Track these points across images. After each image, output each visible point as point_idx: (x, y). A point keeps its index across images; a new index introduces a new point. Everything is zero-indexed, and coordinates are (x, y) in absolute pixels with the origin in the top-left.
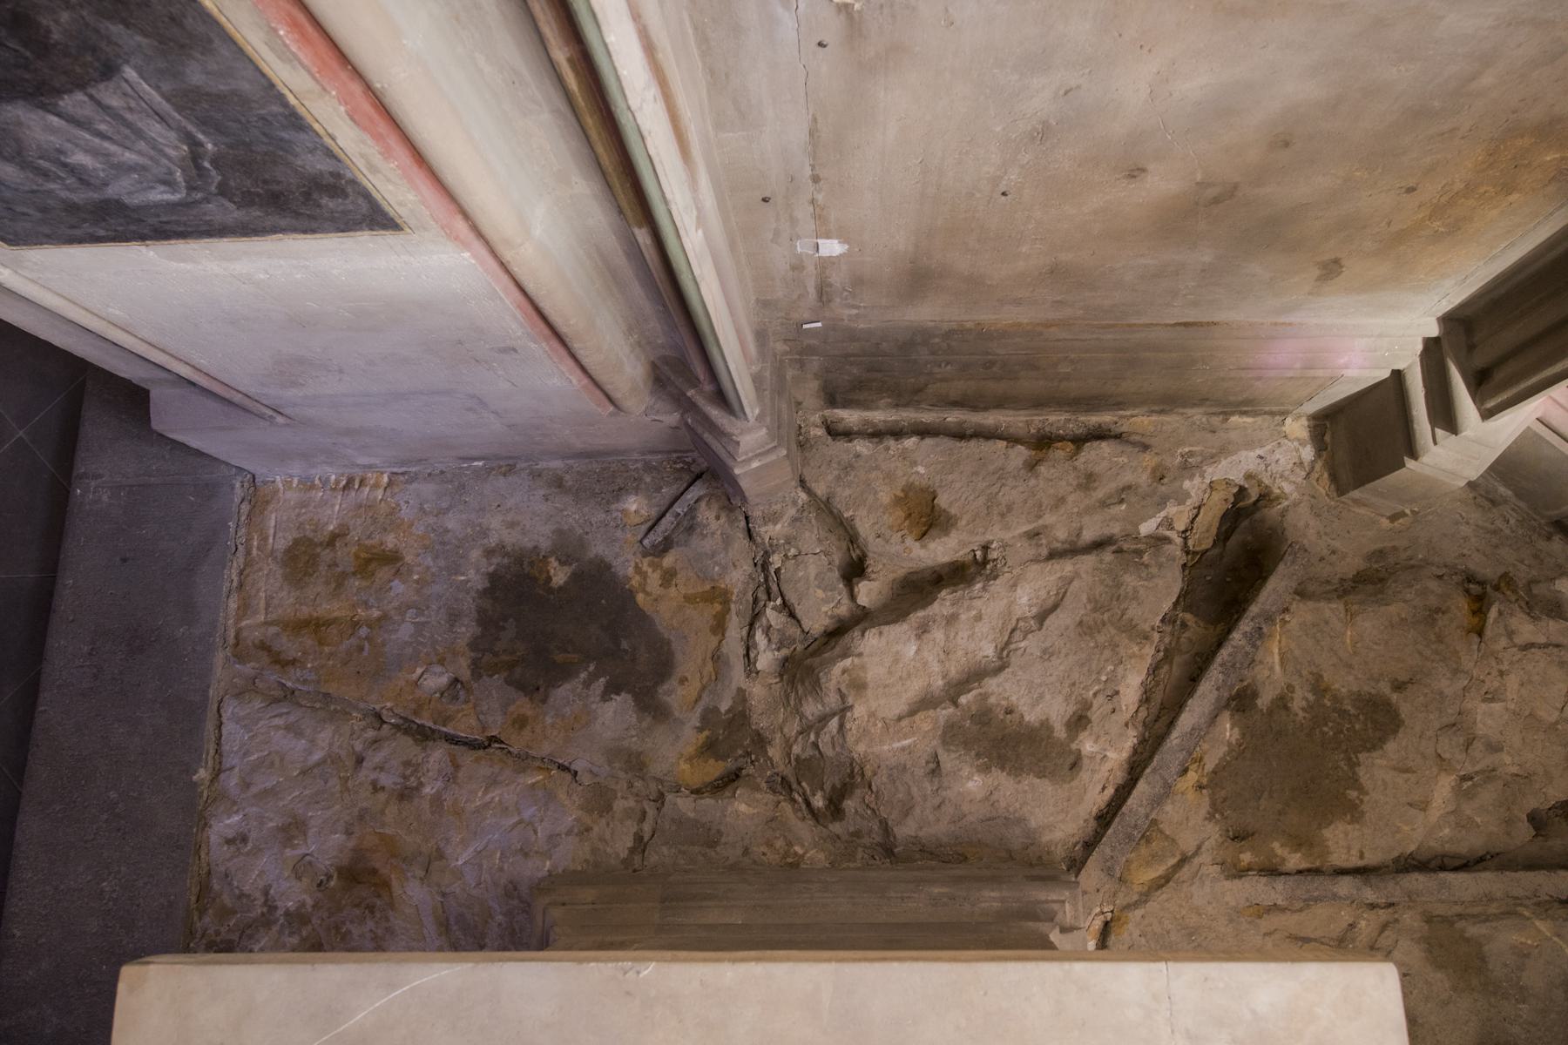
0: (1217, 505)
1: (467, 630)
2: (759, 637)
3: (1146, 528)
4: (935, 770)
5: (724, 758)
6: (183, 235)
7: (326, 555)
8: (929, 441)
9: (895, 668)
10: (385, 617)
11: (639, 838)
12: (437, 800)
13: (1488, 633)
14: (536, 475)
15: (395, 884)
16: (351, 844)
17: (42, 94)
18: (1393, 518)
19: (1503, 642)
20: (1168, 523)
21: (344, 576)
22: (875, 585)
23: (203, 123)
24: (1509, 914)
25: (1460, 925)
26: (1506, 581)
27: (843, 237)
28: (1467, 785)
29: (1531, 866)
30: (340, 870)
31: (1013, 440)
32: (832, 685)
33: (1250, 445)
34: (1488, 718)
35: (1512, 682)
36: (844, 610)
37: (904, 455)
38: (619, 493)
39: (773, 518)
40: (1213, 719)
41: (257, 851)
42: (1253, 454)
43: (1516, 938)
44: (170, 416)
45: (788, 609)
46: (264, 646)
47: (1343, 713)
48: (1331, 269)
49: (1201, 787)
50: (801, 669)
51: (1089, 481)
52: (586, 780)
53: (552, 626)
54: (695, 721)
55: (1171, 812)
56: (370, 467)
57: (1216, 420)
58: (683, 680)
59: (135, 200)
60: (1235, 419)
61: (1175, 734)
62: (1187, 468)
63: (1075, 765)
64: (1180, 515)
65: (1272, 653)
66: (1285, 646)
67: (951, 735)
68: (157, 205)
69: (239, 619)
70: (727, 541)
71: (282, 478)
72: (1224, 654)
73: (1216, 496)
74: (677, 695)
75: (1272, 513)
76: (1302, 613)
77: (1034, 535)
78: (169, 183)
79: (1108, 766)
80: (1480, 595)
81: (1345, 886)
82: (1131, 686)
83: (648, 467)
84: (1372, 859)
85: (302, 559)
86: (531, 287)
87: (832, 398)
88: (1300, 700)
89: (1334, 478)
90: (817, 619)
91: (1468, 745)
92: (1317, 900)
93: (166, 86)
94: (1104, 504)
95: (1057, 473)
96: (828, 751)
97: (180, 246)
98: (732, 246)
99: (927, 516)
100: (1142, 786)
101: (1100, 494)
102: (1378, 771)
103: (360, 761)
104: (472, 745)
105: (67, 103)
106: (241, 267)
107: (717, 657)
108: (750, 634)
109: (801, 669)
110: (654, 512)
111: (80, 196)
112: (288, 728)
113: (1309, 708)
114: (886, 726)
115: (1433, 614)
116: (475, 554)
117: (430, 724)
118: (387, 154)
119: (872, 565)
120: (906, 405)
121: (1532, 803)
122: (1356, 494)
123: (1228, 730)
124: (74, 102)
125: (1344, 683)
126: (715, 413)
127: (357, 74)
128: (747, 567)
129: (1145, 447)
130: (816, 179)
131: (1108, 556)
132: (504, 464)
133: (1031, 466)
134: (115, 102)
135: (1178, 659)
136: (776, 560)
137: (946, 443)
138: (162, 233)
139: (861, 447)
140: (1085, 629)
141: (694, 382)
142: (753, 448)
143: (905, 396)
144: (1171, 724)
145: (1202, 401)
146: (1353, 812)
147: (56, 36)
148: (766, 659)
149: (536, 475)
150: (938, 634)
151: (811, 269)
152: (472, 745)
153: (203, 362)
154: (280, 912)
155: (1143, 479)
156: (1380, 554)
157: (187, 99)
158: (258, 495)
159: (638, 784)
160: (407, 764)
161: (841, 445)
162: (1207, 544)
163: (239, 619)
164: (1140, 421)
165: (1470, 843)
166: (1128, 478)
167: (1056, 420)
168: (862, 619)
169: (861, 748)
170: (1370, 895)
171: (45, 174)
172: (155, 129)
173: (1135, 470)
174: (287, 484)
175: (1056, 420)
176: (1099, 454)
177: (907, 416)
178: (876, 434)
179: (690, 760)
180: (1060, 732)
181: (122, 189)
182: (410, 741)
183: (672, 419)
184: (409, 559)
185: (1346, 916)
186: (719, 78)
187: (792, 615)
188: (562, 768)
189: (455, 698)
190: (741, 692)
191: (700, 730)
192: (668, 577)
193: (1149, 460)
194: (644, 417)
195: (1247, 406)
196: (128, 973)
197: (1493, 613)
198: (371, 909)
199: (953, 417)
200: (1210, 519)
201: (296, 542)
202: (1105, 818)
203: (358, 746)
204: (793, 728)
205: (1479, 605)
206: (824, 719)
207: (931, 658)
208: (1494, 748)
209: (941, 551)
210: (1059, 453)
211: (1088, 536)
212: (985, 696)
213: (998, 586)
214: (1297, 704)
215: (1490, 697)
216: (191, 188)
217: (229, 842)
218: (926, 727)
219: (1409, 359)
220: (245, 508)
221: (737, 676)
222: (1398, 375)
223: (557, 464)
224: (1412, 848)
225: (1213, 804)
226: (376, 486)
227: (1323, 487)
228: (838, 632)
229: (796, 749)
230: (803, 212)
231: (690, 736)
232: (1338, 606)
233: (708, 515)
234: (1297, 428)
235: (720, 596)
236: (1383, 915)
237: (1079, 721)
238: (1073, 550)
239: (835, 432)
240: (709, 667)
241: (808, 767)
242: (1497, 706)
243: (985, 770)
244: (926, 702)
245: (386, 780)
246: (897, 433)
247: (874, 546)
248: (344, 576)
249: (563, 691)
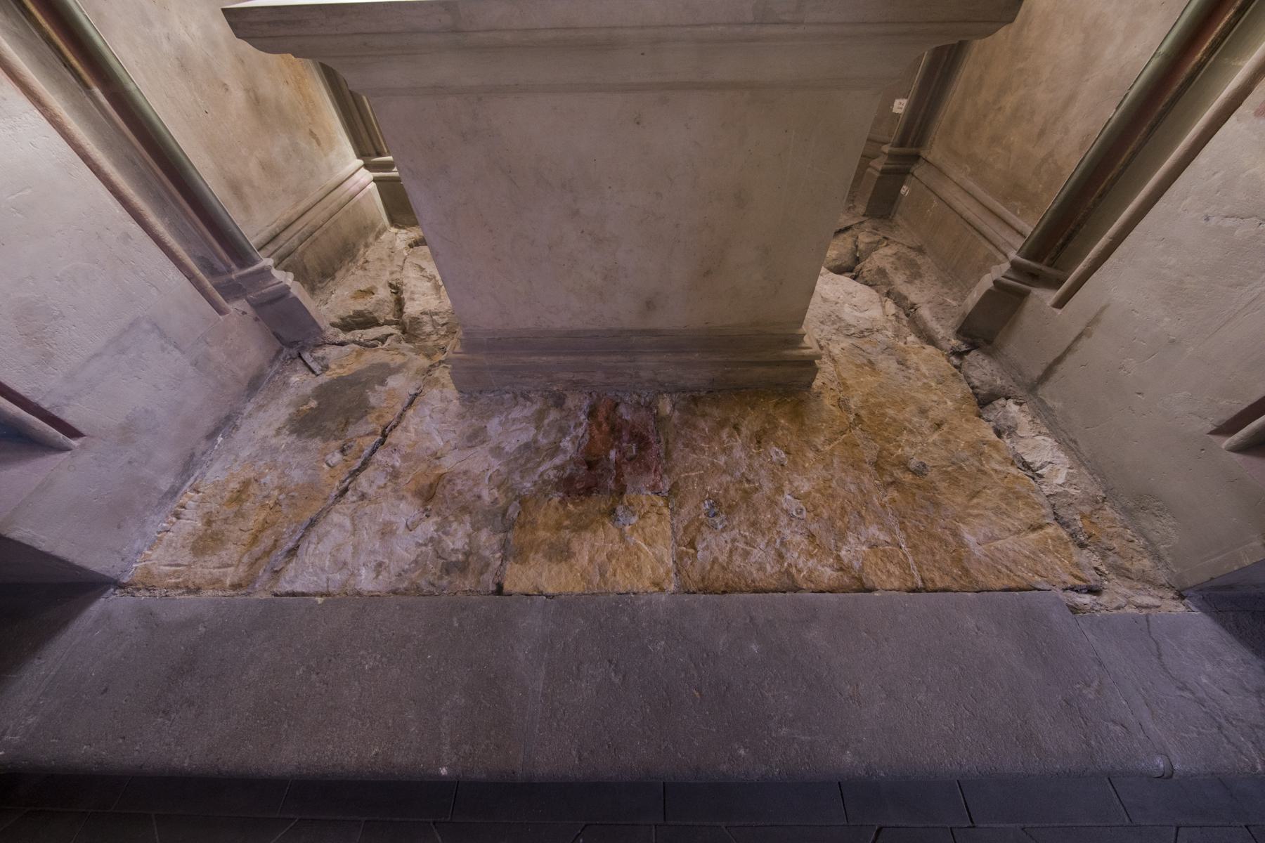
12: (405, 458)
15: (441, 472)
16: (410, 498)
30: (424, 505)
41: (391, 554)
154: (435, 535)
188: (411, 403)
198: (450, 481)
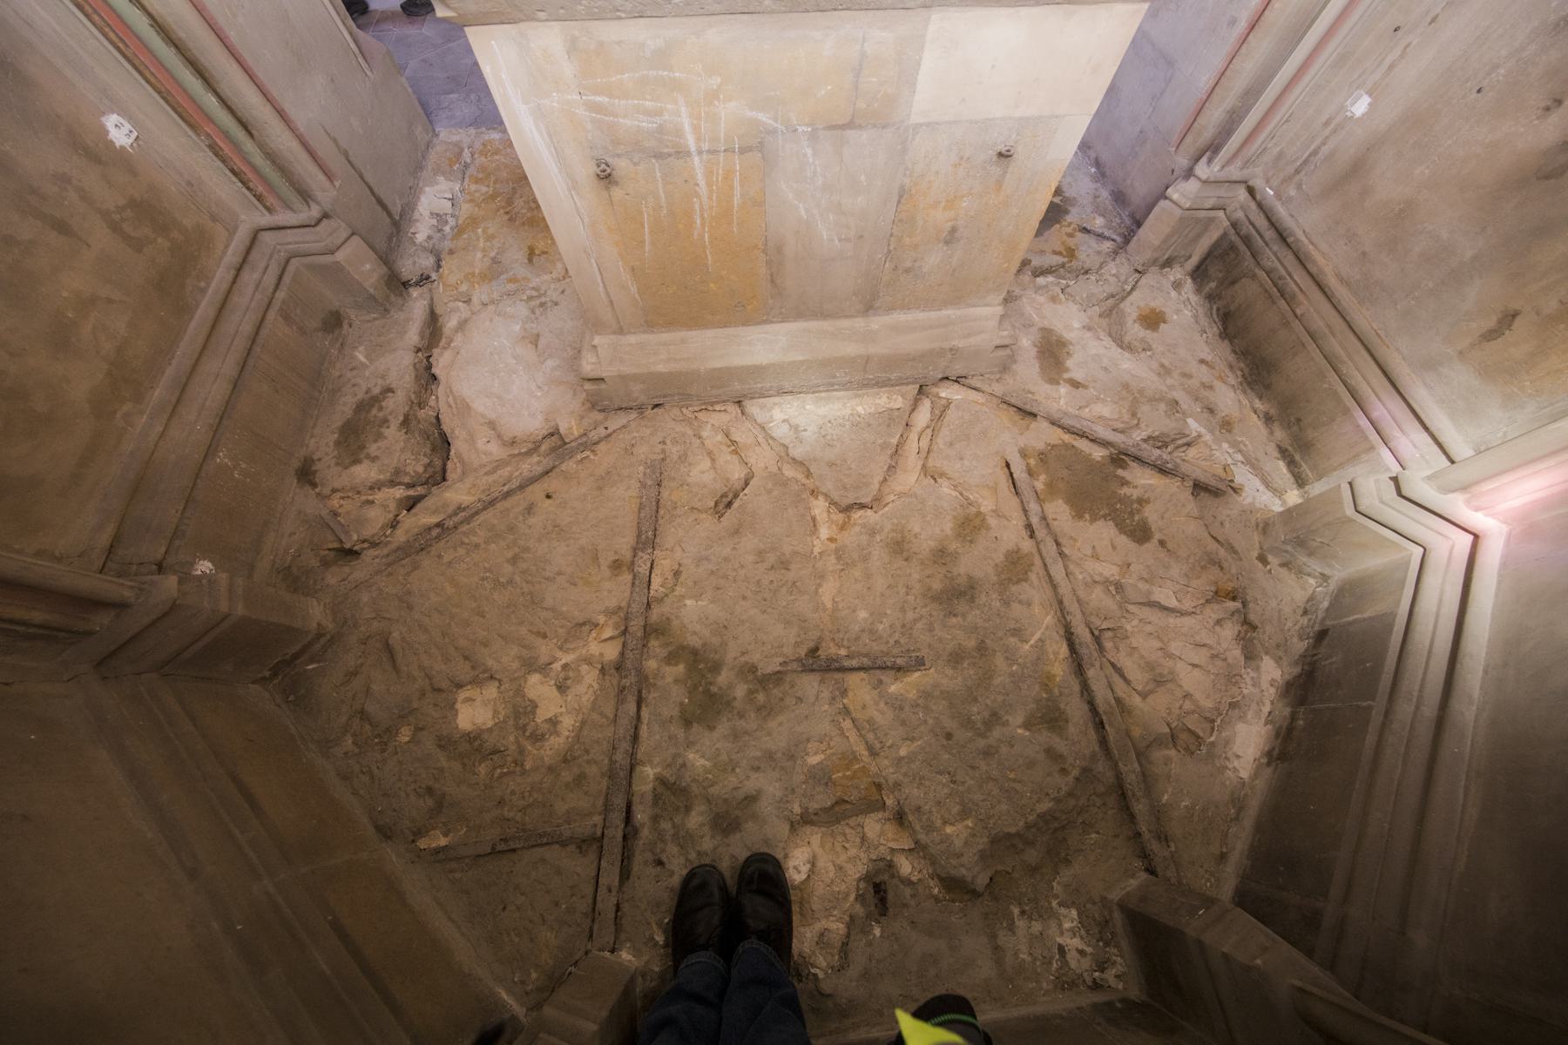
19: (1215, 616)
47: (1132, 514)
60: (1282, 464)
102: (1102, 533)
146: (1079, 515)
150: (1088, 334)
180: (1066, 376)
237: (1075, 384)
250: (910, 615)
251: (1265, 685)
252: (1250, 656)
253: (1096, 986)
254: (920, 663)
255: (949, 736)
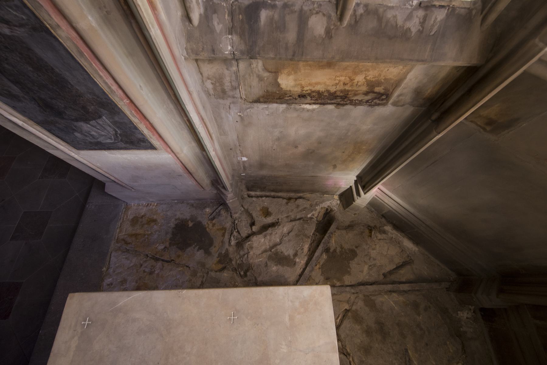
0: (323, 212)
1: (169, 236)
2: (232, 238)
3: (309, 216)
4: (266, 265)
5: (222, 264)
6: (113, 149)
7: (140, 220)
8: (268, 198)
9: (260, 244)
10: (152, 233)
11: (202, 282)
12: (158, 274)
13: (372, 237)
14: (188, 204)
17: (86, 121)
18: (355, 214)
20: (313, 215)
21: (144, 224)
22: (256, 227)
23: (118, 127)
24: (380, 294)
25: (370, 297)
26: (375, 227)
27: (246, 157)
28: (371, 267)
29: (383, 284)
31: (284, 198)
32: (246, 248)
33: (328, 200)
34: (373, 253)
35: (378, 247)
36: (250, 232)
37: (263, 201)
38: (205, 207)
39: (236, 213)
40: (321, 254)
42: (329, 202)
43: (381, 299)
44: (110, 189)
45: (238, 232)
46: (123, 240)
48: (335, 167)
49: (319, 268)
50: (240, 245)
51: (298, 206)
52: (192, 269)
53: (188, 235)
54: (217, 255)
55: (314, 273)
56: (153, 201)
57: (322, 195)
58: (215, 247)
59: (104, 142)
60: (325, 195)
61: (314, 257)
62: (317, 204)
63: (295, 264)
64: (316, 213)
65: (333, 241)
66: (335, 239)
67: (270, 258)
68: (108, 143)
69: (119, 234)
70: (226, 218)
71: (133, 204)
72: (323, 241)
73: (323, 210)
74: (213, 250)
75: (333, 213)
76: (338, 233)
77: (287, 217)
78: (111, 139)
79: (301, 264)
80: (371, 229)
81: (348, 289)
82: (306, 247)
83: (211, 202)
84: (353, 283)
85: (135, 221)
86: (183, 162)
87: (249, 189)
88: (338, 250)
89: (343, 207)
90: (244, 233)
91: (370, 259)
92: (343, 292)
93: (111, 120)
94: (301, 211)
95: (292, 205)
96: (245, 262)
97: (112, 151)
98: (225, 158)
99: (266, 213)
100: (308, 268)
101: (300, 209)
102: (353, 264)
103: (141, 265)
104: (167, 262)
105: (91, 122)
106: (125, 156)
107: (223, 242)
108: (230, 237)
109: (240, 245)
110: (212, 211)
111: (93, 141)
112: (126, 258)
113: (340, 252)
114: (257, 256)
115: (362, 233)
116: (173, 220)
117: (158, 257)
118: (154, 135)
119: (256, 223)
120: (263, 191)
121: (383, 271)
122: (347, 209)
123: (325, 256)
124: (93, 122)
125: (347, 246)
126: (223, 190)
127: (148, 120)
128: (230, 223)
129: (309, 200)
130: (240, 146)
131: (301, 221)
132: (181, 201)
133: (287, 203)
134: (101, 123)
135: (315, 242)
136: (236, 222)
137: (271, 198)
138: (109, 148)
139: (254, 199)
140: (297, 236)
141: (219, 184)
142: (230, 197)
143: (263, 189)
144: (313, 255)
145: (318, 191)
146: (349, 273)
147: (90, 110)
148: (233, 242)
149: (188, 204)
150: (268, 237)
151: (241, 163)
152: (167, 262)
153: (116, 176)
155: (308, 206)
156: (353, 221)
157: (115, 123)
158: (127, 207)
159: (203, 270)
160: (152, 266)
161: (250, 199)
162: (321, 219)
163: (119, 234)
164: (308, 195)
165: (372, 279)
166: (305, 206)
167: (292, 195)
168: (254, 234)
169: (251, 261)
170: (353, 291)
171: (86, 136)
172: (108, 128)
173: (306, 204)
174: (134, 205)
175: (292, 195)
176: (300, 201)
177: (263, 193)
178: (257, 197)
179: (215, 264)
180: (292, 257)
181: (101, 139)
182: (153, 261)
183: (215, 192)
184: (158, 221)
185: (349, 296)
186: (220, 127)
187: (239, 233)
188: (187, 266)
189: (165, 251)
190: (227, 249)
191: (218, 257)
192: (214, 225)
193: (309, 202)
194: (209, 192)
195: (327, 193)
196: (70, 295)
197: (373, 233)
199: (273, 194)
200: (321, 214)
201: (134, 217)
202: (300, 276)
203: (142, 262)
204: (238, 257)
205: (371, 231)
206: (244, 255)
207: (267, 242)
208: (374, 259)
209: (270, 220)
210: (292, 201)
211: (298, 217)
212: (277, 250)
213: (280, 227)
214: (338, 251)
215: (374, 249)
216: (115, 140)
217: (108, 285)
218: (265, 256)
219: (352, 184)
220: (124, 210)
221: (227, 246)
222: (351, 187)
223: (192, 202)
224: (361, 281)
225: (322, 272)
226: (154, 205)
227: (342, 208)
228: (248, 237)
229: (238, 262)
230: (238, 152)
231: (215, 259)
232: (344, 231)
233: (223, 212)
234: (336, 197)
235: (224, 229)
236: (356, 295)
237: (296, 255)
238: (295, 220)
239: (249, 196)
240: (221, 244)
241: (240, 266)
242: (374, 251)
243: (276, 265)
244: (265, 251)
245: (147, 270)
246: (262, 197)
247: (256, 219)
248: (144, 224)
249: (189, 249)
250: (391, 351)
251: (392, 232)
252: (384, 232)
253: (474, 312)
254: (406, 350)
255: (427, 344)
